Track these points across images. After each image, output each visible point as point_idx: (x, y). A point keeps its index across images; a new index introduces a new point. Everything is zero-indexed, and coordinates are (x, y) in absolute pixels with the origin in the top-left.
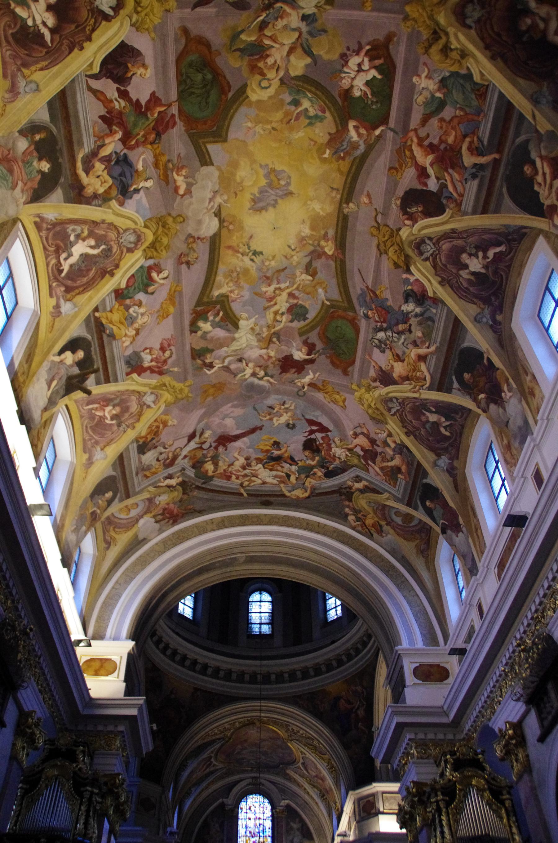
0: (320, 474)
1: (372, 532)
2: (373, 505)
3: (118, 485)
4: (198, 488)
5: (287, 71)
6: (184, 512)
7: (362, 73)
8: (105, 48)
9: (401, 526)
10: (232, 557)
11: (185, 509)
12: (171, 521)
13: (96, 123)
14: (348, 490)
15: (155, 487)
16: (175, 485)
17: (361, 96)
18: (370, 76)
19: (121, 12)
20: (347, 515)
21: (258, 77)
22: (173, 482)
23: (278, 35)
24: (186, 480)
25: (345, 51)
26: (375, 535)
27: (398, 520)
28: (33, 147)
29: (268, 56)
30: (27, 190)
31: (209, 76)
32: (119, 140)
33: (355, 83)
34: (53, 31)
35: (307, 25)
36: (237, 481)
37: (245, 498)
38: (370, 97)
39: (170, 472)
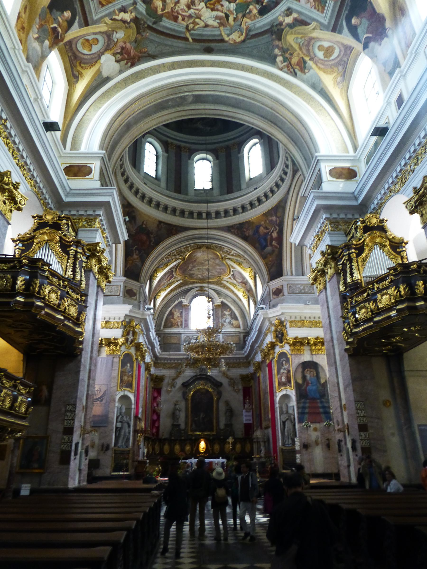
0: (255, 11)
1: (296, 70)
2: (299, 40)
3: (76, 6)
4: (150, 28)
6: (140, 55)
9: (322, 60)
10: (182, 95)
11: (141, 53)
12: (129, 64)
14: (279, 27)
15: (111, 19)
16: (129, 21)
20: (276, 56)
22: (127, 17)
24: (139, 16)
26: (299, 73)
27: (320, 54)
36: (183, 22)
37: (190, 43)
39: (124, 4)
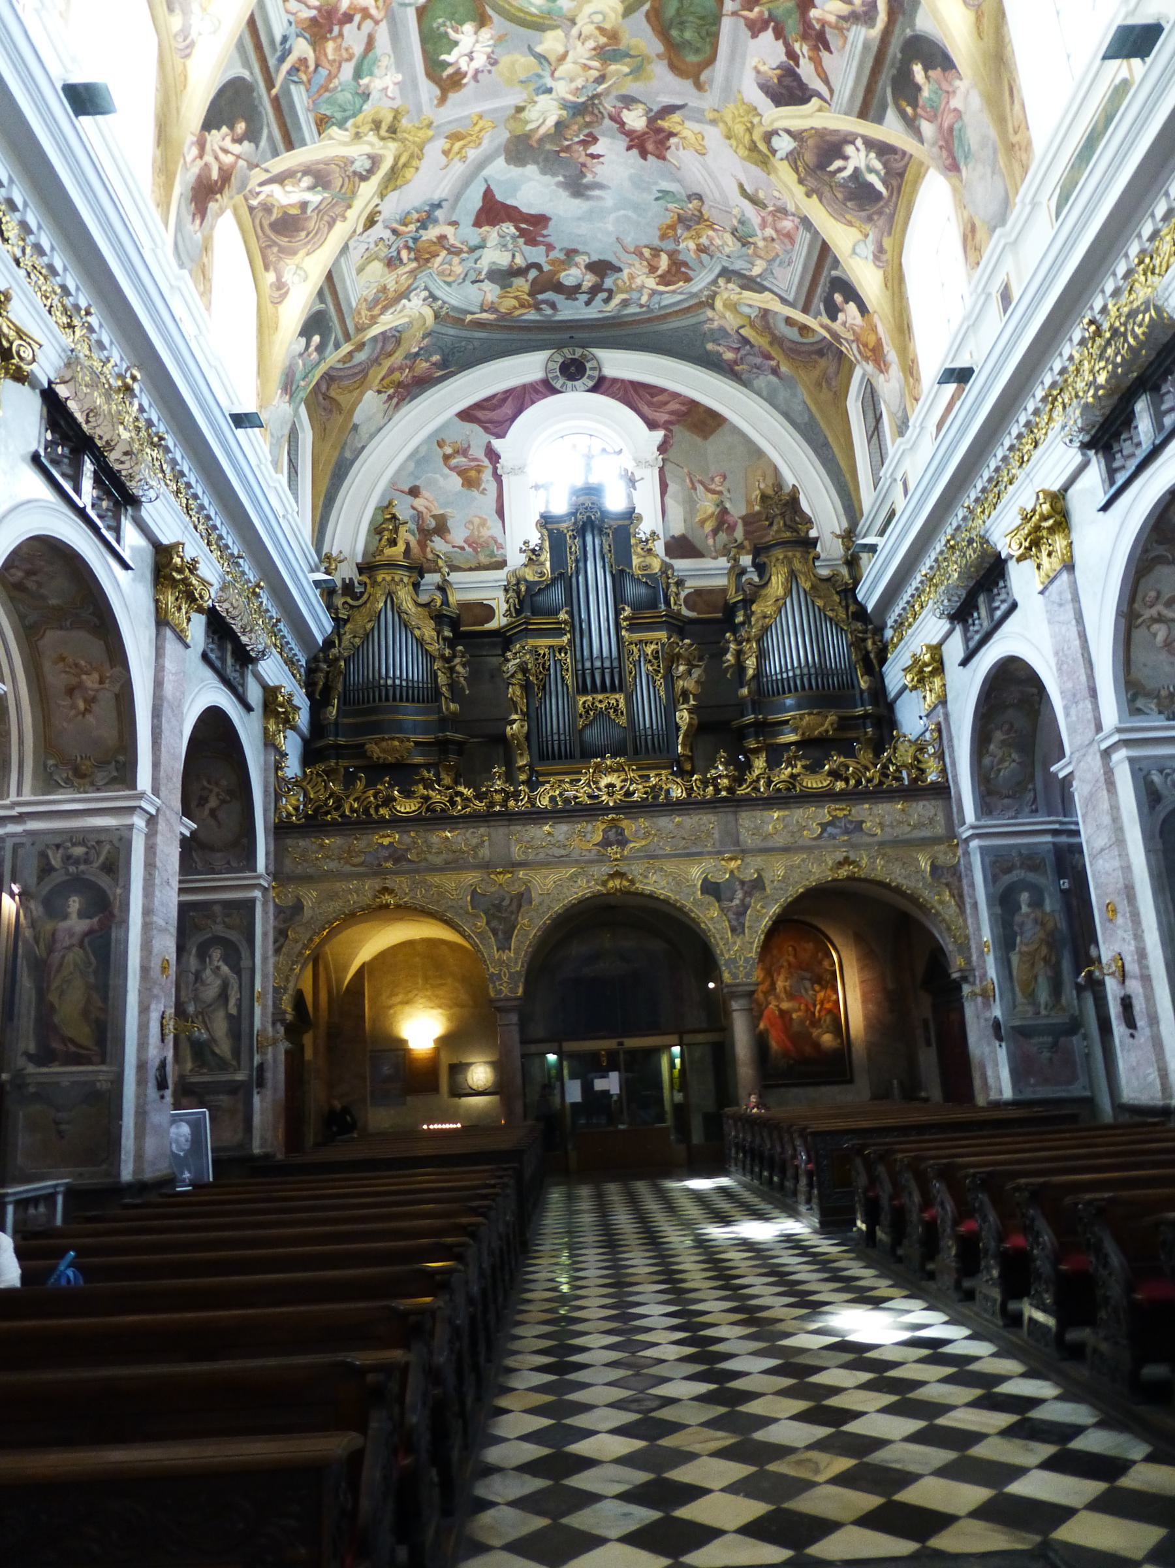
5: (567, 35)
7: (467, 51)
8: (797, 113)
13: (839, 51)
17: (461, 24)
18: (456, 52)
19: (769, 129)
21: (607, 26)
23: (581, 73)
25: (493, 69)
28: (919, 111)
29: (594, 49)
30: (950, 84)
31: (674, 33)
32: (814, 6)
33: (473, 38)
34: (853, 143)
35: (545, 84)
38: (450, 31)
